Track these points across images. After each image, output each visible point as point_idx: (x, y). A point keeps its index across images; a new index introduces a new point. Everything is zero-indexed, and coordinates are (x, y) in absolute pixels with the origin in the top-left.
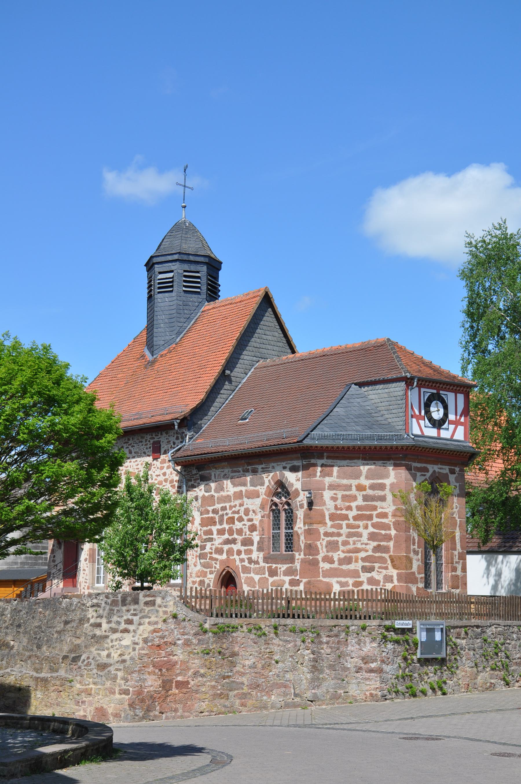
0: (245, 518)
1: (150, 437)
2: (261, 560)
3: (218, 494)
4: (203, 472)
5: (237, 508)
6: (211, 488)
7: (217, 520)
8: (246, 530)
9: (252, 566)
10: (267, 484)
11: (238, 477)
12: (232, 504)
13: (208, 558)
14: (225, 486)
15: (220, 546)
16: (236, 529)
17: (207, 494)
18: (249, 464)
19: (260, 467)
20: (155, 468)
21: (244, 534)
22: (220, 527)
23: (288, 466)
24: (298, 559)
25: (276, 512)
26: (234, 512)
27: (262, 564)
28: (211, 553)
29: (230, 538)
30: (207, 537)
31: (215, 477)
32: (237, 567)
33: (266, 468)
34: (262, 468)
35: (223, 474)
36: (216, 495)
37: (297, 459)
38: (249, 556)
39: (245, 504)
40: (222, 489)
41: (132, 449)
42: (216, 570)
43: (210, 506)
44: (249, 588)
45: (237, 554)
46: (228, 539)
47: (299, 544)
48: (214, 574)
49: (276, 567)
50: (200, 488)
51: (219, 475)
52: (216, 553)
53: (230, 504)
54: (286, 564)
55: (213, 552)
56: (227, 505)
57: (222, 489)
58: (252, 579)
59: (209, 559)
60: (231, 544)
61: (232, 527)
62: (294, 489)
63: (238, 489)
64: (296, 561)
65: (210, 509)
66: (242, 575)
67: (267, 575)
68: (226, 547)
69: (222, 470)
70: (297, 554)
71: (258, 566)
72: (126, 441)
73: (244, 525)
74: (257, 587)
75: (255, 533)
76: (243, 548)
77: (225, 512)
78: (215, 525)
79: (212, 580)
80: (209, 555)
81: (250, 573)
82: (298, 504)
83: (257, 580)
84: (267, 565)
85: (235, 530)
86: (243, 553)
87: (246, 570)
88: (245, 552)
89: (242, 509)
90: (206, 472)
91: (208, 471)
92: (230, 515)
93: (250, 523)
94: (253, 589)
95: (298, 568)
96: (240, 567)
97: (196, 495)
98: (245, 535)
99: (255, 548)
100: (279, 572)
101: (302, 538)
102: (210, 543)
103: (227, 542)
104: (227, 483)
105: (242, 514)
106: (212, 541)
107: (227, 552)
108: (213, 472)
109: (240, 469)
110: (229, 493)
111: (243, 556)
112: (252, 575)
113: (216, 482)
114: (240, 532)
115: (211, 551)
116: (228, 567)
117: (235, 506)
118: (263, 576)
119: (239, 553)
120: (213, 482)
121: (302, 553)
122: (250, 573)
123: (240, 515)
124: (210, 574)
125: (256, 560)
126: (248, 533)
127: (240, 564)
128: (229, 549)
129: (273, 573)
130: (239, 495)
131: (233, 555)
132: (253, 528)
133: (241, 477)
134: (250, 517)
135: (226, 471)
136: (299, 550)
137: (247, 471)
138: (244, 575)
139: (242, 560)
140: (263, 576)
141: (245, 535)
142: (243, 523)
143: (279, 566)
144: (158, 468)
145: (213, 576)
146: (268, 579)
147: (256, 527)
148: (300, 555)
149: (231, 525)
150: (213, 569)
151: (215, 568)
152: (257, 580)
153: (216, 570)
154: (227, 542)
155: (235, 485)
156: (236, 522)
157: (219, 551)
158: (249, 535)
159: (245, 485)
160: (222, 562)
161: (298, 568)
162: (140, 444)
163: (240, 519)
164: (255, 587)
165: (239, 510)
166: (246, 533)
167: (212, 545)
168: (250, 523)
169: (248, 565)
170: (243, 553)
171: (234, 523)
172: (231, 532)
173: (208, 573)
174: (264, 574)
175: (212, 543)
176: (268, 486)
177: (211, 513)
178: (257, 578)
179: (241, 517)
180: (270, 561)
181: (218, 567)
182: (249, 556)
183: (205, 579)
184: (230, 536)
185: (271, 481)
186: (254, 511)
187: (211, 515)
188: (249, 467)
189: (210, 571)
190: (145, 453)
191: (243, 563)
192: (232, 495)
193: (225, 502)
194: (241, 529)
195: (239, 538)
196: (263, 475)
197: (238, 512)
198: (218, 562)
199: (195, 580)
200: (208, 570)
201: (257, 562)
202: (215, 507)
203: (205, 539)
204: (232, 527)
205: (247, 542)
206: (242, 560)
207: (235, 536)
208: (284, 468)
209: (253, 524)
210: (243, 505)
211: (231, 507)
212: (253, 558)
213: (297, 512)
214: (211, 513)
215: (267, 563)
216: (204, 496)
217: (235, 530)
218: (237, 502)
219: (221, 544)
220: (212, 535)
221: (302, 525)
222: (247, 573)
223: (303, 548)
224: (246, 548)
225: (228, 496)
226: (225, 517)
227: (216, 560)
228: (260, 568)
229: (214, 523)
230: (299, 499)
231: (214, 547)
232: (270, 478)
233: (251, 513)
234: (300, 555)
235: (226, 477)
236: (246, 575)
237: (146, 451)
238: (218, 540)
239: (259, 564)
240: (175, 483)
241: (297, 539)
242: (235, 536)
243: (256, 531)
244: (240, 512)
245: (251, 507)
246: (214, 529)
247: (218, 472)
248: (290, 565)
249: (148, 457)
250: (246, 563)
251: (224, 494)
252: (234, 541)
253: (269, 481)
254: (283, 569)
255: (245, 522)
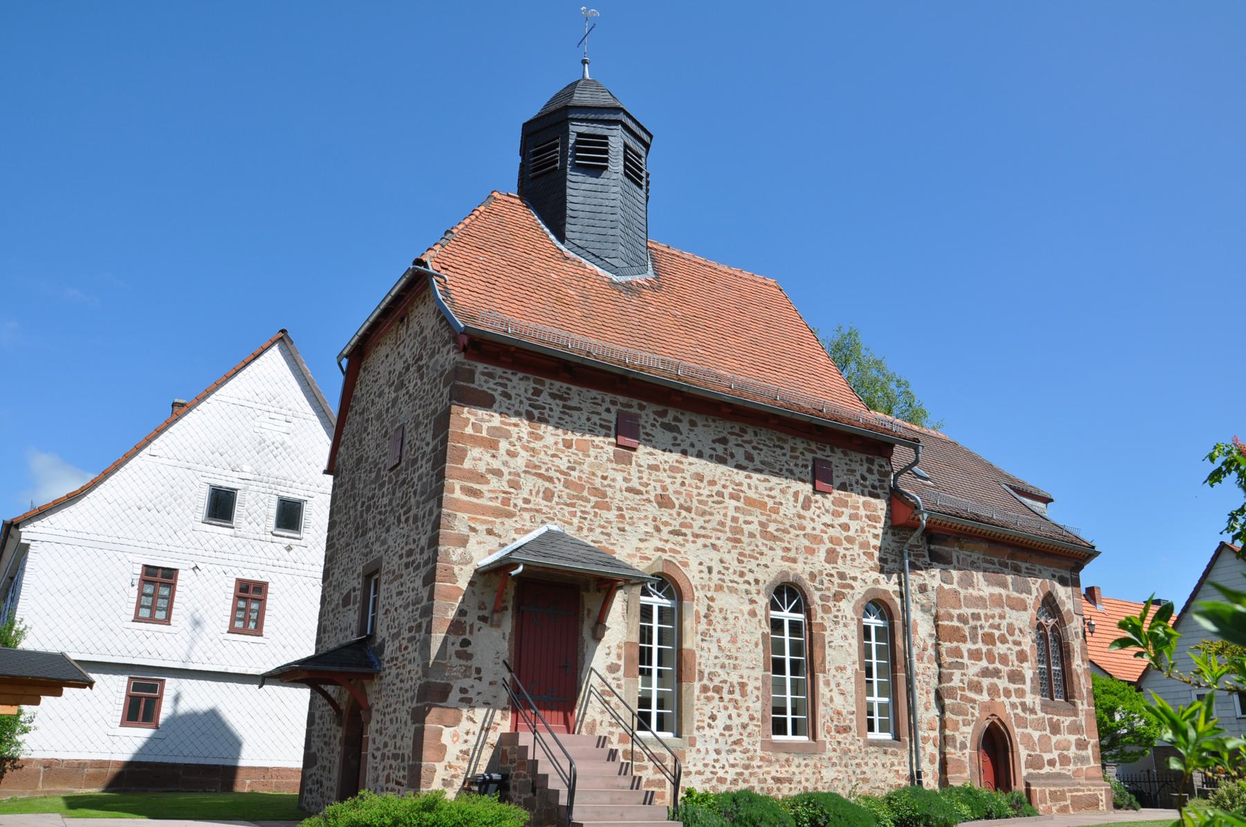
0: (1010, 638)
1: (805, 445)
2: (1038, 708)
3: (965, 591)
4: (937, 547)
5: (997, 621)
6: (953, 578)
7: (967, 634)
8: (1013, 657)
9: (1028, 716)
10: (1035, 593)
11: (994, 572)
12: (989, 612)
13: (959, 697)
14: (975, 580)
15: (976, 679)
16: (999, 654)
17: (946, 587)
18: (1011, 557)
19: (1023, 565)
20: (819, 508)
21: (1010, 663)
22: (974, 647)
23: (1057, 575)
24: (1082, 711)
25: (1042, 638)
26: (992, 626)
27: (1041, 714)
28: (963, 689)
29: (991, 667)
30: (954, 660)
31: (958, 561)
32: (1008, 715)
33: (1031, 569)
34: (1027, 568)
35: (969, 560)
36: (962, 592)
37: (1066, 568)
38: (1022, 700)
39: (1007, 616)
40: (971, 585)
41: (755, 453)
42: (974, 718)
43: (954, 608)
44: (1028, 752)
45: (1005, 696)
46: (987, 668)
47: (1080, 688)
48: (972, 726)
49: (1058, 720)
50: (933, 573)
51: (964, 560)
52: (970, 689)
53: (985, 611)
54: (1069, 716)
55: (966, 686)
56: (982, 612)
57: (971, 584)
58: (1030, 736)
59: (960, 699)
60: (992, 677)
61: (992, 649)
62: (1066, 609)
63: (997, 590)
64: (1080, 712)
65: (955, 612)
66: (1016, 730)
67: (1048, 732)
68: (986, 682)
69: (969, 553)
70: (1078, 702)
71: (1034, 717)
72: (737, 430)
73: (1009, 649)
74: (1038, 750)
75: (1025, 665)
76: (1012, 687)
77: (978, 623)
78: (965, 641)
79: (969, 737)
80: (959, 692)
81: (1026, 728)
82: (1073, 631)
83: (1036, 739)
84: (1047, 716)
85: (997, 656)
86: (1013, 694)
87: (1022, 723)
88: (1016, 694)
89: (1004, 623)
90: (943, 548)
91: (947, 549)
92: (986, 630)
93: (1017, 648)
94: (1033, 753)
95: (1084, 723)
96: (1012, 716)
97: (921, 582)
98: (1013, 665)
99: (1027, 687)
100: (1062, 728)
101: (1083, 680)
102: (960, 671)
103: (985, 673)
104: (978, 576)
105: (1004, 631)
106: (963, 669)
107: (989, 690)
108: (955, 552)
109: (996, 560)
110: (981, 593)
111: (1014, 699)
112: (1029, 730)
113: (959, 569)
114: (1004, 659)
115: (961, 685)
116: (993, 715)
117: (993, 617)
118: (1044, 733)
119: (1007, 693)
120: (955, 568)
121: (1085, 702)
122: (1026, 728)
123: (1002, 632)
124: (964, 725)
125: (1031, 707)
126: (1016, 663)
127: (1011, 712)
128: (992, 684)
129: (1055, 729)
130: (997, 601)
131: (1000, 697)
132: (1022, 657)
133: (998, 573)
134: (1016, 638)
135: (975, 556)
136: (1081, 698)
137: (1006, 566)
138: (1019, 730)
139: (1013, 706)
140: (1044, 733)
141: (1013, 665)
142: (1007, 645)
143: (1062, 718)
144: (827, 511)
145: (969, 729)
146: (1050, 737)
147: (1026, 656)
148: (1082, 704)
149: (990, 647)
150: (969, 717)
151: (973, 715)
152: (1036, 739)
153: (974, 718)
154: (985, 673)
155: (990, 583)
156: (998, 644)
157: (977, 688)
158: (1018, 666)
159: (1004, 585)
160: (984, 707)
161: (1084, 723)
162: (779, 451)
163: (1003, 640)
164: (1035, 751)
165: (999, 625)
166: (1012, 662)
167: (963, 674)
168: (1017, 648)
169: (1022, 714)
170: (1013, 694)
171: (994, 644)
172: (990, 657)
173: (961, 722)
174: (1045, 730)
175: (963, 671)
176: (1037, 597)
177: (955, 619)
178: (1036, 735)
179: (1003, 635)
180: (1049, 710)
181: (977, 713)
182: (1022, 700)
183: (957, 734)
184: (989, 663)
185: (1040, 590)
186: (1021, 631)
187: (956, 623)
188: (1009, 562)
189: (964, 720)
190: (791, 472)
191: (1015, 711)
192: (987, 598)
193: (977, 606)
194: (1006, 655)
195: (1005, 669)
196: (1029, 579)
197: (998, 627)
198: (977, 706)
199: (926, 735)
200: (960, 718)
201: (1033, 711)
202: (961, 611)
203: (950, 664)
204: (992, 649)
205: (1016, 677)
206: (1013, 706)
207: (998, 665)
208: (1054, 576)
209: (1022, 650)
210: (1004, 618)
211: (987, 617)
212: (1027, 704)
213: (1073, 643)
214: (955, 619)
215: (1047, 713)
216: (940, 589)
217: (997, 656)
218: (997, 611)
219: (977, 676)
220: (962, 657)
221: (1079, 662)
222: (1023, 728)
223: (1085, 695)
224: (1017, 686)
225: (981, 597)
226: (980, 632)
227: (974, 701)
228: (1038, 720)
229: (963, 639)
230: (1073, 625)
231: (966, 679)
232: (1038, 585)
233: (1017, 632)
234: (1082, 704)
235: (974, 566)
236: (1021, 730)
237: (797, 471)
238: (974, 668)
239: (1036, 713)
240: (872, 550)
241: (1077, 681)
242: (998, 665)
243: (1027, 661)
244: (1002, 627)
245: (1017, 624)
246: (965, 647)
247: (963, 554)
248: (1074, 718)
249: (800, 483)
250: (1019, 711)
251: (975, 593)
252: (996, 673)
253: (1037, 589)
254: (1067, 723)
255: (1010, 645)
